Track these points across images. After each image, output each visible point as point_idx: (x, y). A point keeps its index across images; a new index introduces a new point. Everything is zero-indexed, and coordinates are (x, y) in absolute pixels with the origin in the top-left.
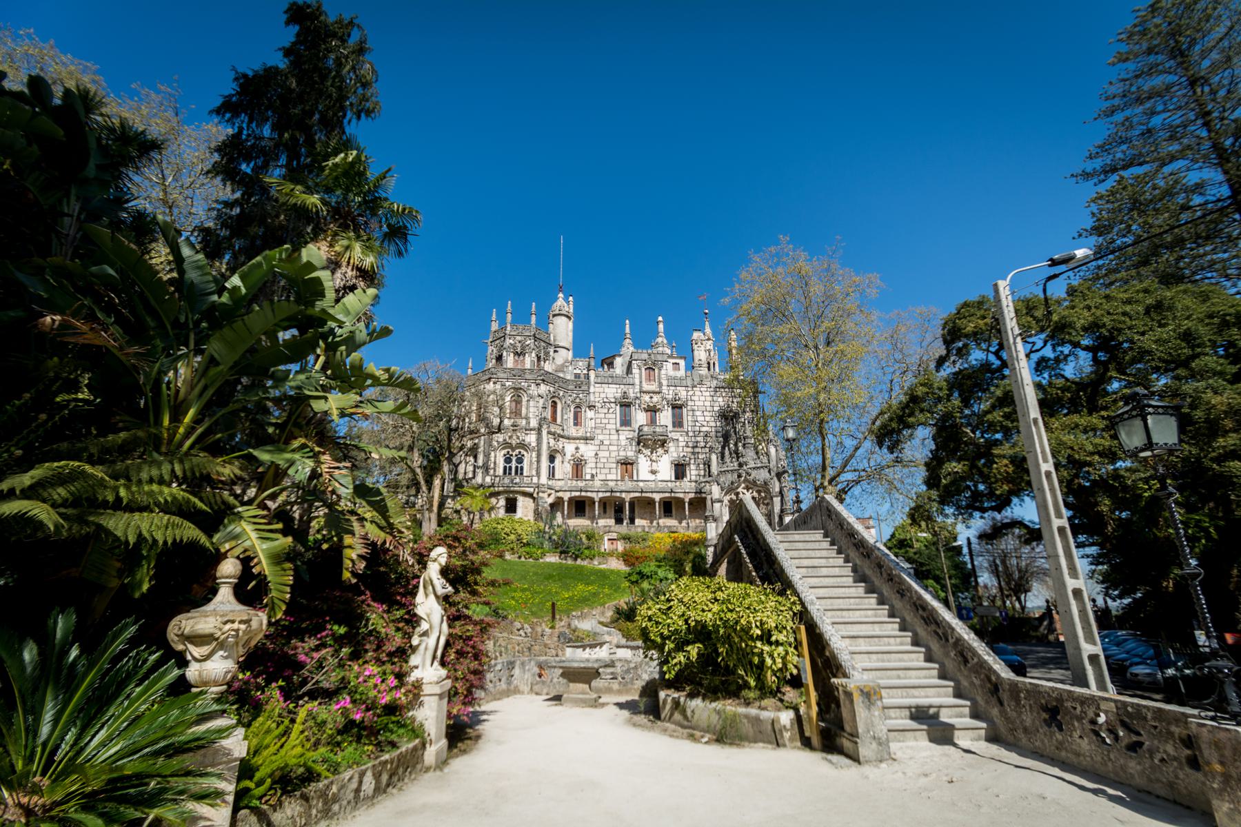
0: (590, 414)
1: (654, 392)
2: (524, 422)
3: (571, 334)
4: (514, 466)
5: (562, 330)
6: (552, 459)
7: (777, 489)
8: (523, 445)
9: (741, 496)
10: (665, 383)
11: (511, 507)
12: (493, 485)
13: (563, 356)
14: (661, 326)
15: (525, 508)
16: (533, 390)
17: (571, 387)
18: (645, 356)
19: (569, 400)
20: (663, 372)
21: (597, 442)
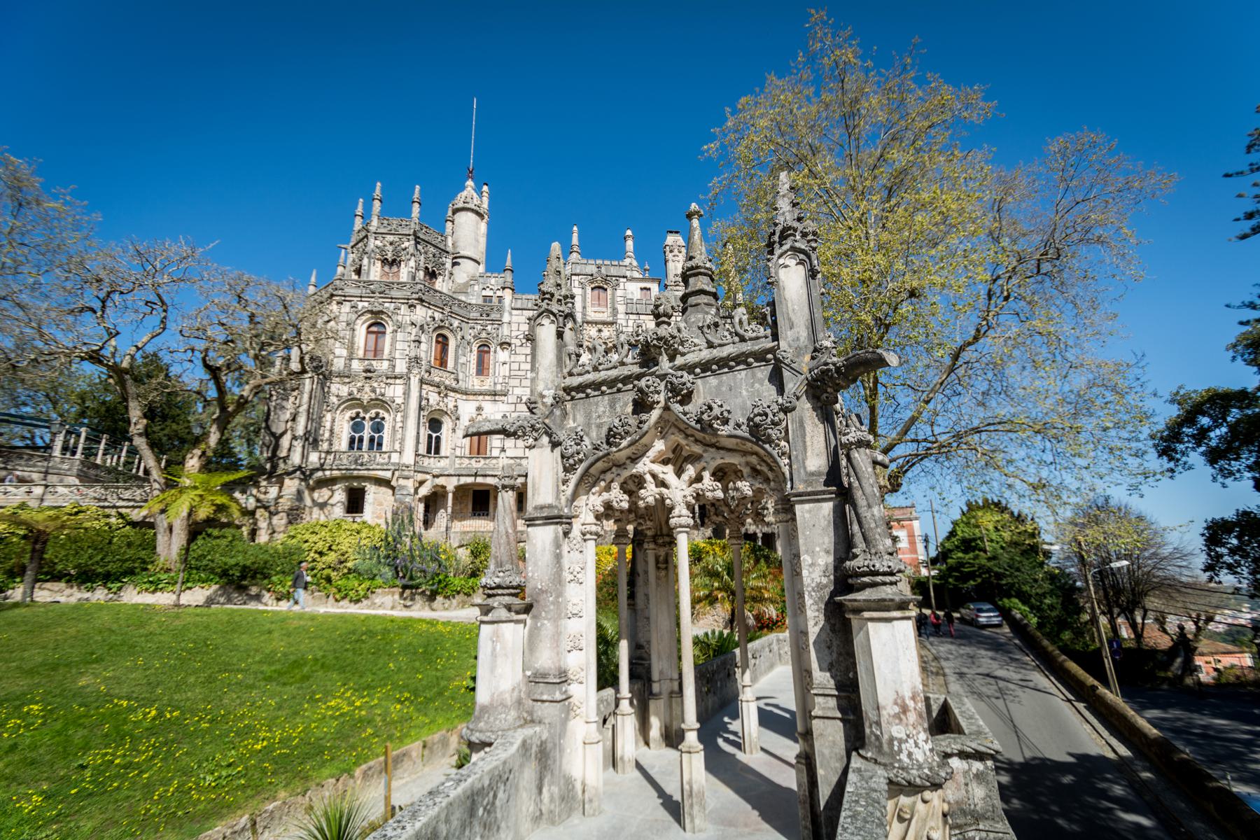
0: (503, 355)
1: (604, 323)
2: (385, 364)
3: (483, 241)
4: (367, 435)
5: (469, 233)
6: (435, 424)
7: (816, 461)
8: (381, 402)
9: (649, 493)
10: (621, 309)
11: (355, 503)
12: (322, 468)
13: (466, 271)
14: (630, 244)
15: (378, 504)
16: (404, 315)
17: (473, 315)
18: (592, 269)
19: (469, 334)
20: (619, 293)
21: (512, 399)
